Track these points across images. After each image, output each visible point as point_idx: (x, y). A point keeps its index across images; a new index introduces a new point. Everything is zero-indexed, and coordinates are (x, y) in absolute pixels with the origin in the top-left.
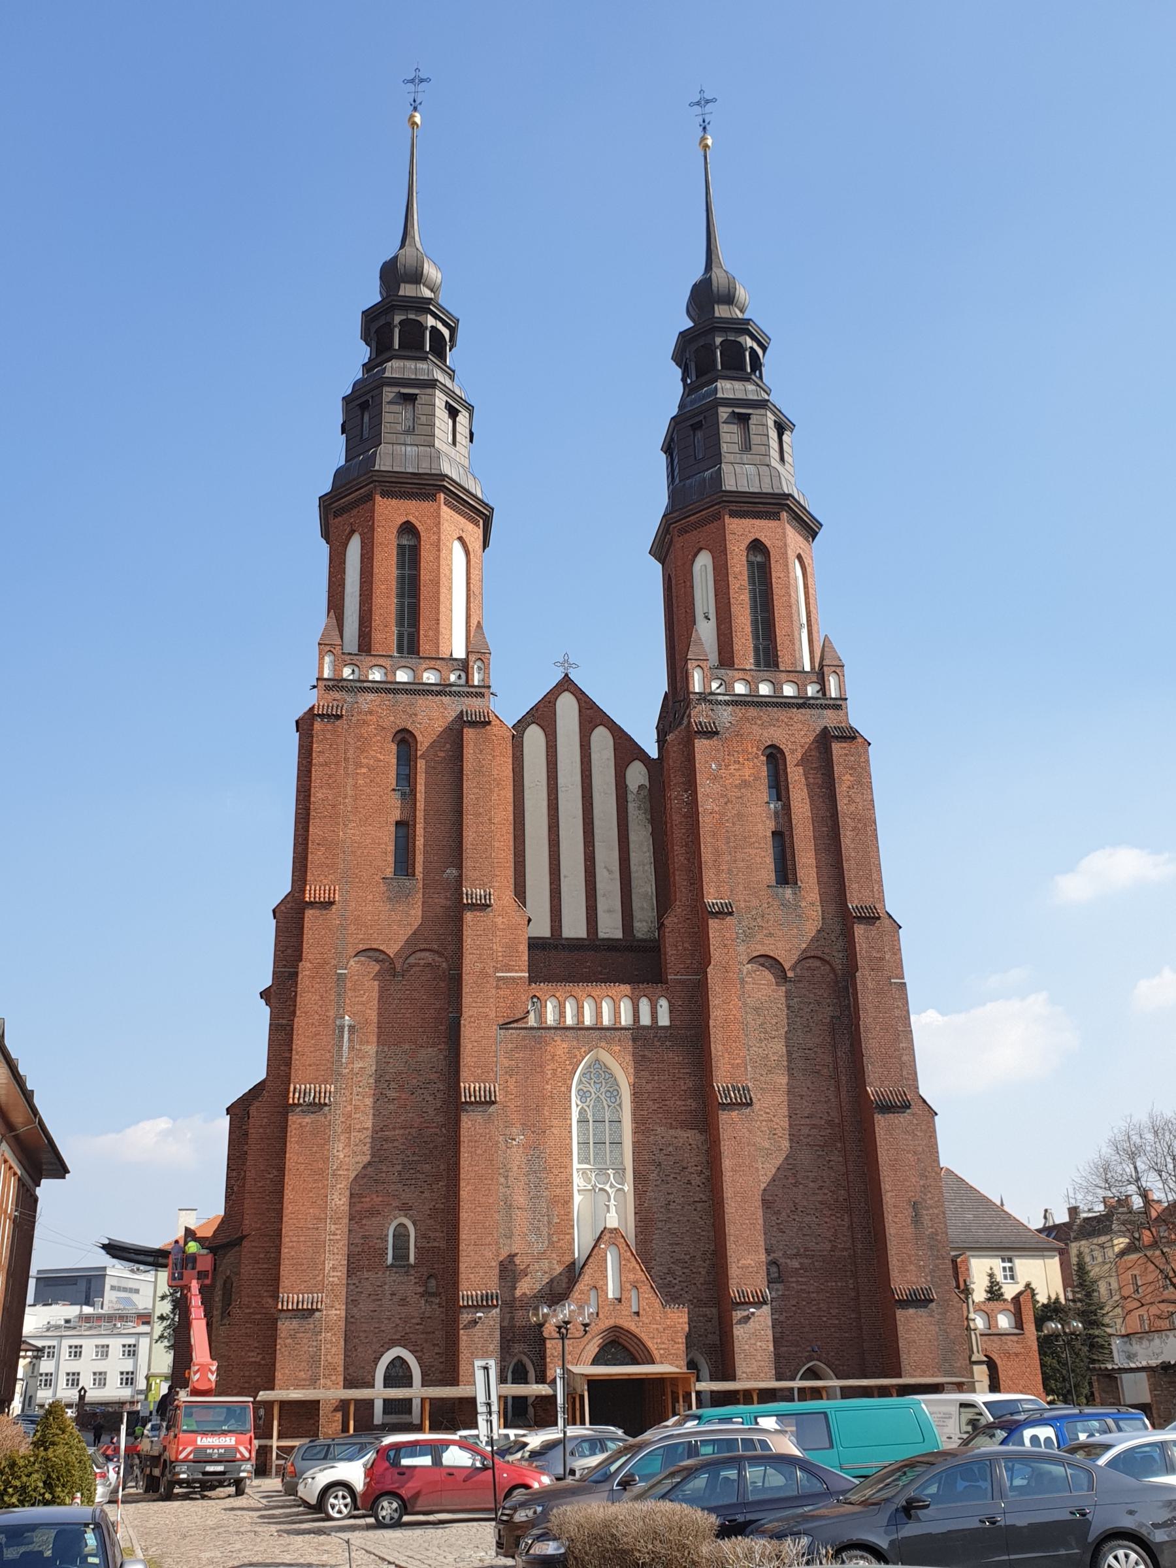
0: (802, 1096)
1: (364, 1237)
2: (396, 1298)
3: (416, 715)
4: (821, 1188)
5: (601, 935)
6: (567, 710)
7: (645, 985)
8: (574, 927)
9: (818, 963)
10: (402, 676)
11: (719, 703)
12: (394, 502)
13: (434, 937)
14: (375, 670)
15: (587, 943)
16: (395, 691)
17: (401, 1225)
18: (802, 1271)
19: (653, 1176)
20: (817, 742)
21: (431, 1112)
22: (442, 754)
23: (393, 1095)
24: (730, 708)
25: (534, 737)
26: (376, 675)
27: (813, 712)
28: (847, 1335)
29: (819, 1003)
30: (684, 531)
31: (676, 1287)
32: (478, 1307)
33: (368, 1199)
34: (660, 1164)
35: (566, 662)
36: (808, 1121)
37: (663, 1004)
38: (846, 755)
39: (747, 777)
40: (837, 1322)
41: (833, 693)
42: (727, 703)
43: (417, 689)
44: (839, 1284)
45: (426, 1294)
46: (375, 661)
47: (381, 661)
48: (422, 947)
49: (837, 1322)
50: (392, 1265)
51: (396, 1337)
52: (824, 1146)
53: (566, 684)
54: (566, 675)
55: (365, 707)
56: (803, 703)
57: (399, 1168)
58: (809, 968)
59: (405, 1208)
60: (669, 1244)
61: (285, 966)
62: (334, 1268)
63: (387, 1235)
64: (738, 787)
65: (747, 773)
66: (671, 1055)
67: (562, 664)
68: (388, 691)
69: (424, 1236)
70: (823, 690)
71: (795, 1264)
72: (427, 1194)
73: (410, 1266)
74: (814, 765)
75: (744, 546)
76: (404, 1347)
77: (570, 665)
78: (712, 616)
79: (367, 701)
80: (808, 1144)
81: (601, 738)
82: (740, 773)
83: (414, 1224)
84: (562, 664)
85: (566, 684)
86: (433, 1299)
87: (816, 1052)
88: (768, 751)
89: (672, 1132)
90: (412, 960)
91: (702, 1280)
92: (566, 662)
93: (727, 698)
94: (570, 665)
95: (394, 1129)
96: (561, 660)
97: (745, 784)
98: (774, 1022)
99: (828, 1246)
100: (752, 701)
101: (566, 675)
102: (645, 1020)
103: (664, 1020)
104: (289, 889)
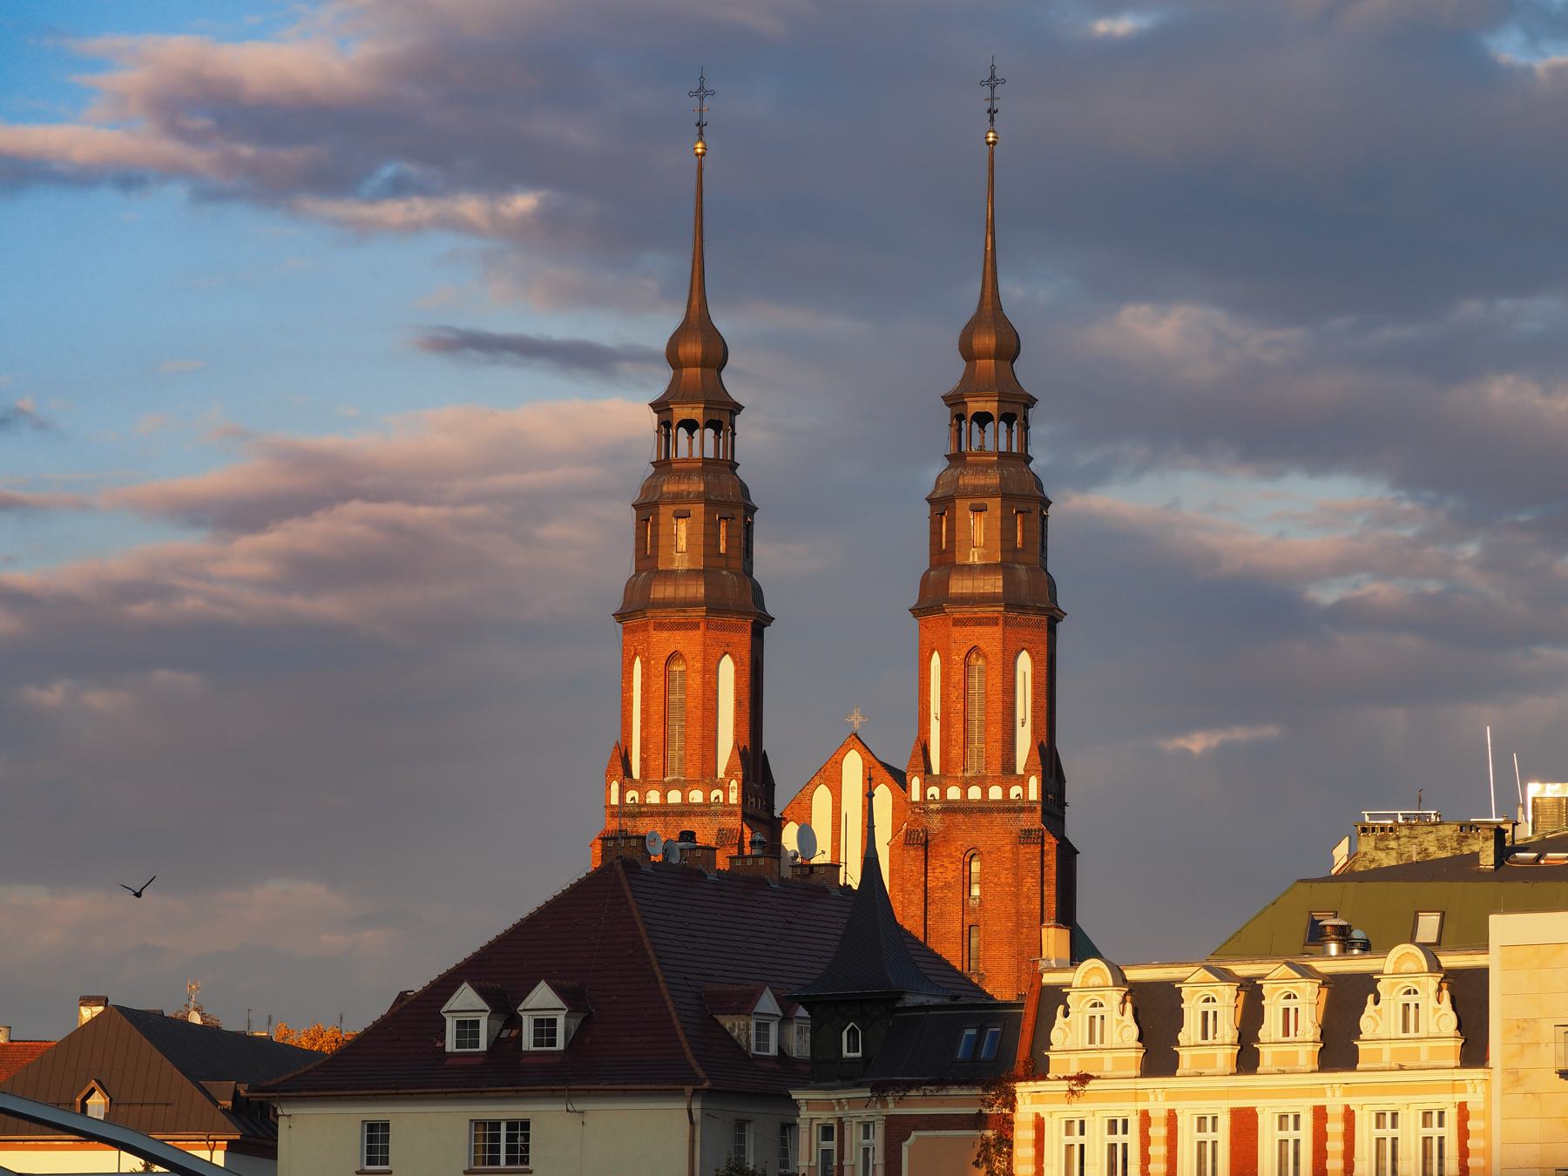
6: (853, 765)
10: (675, 797)
12: (665, 634)
16: (665, 814)
25: (822, 796)
26: (654, 797)
38: (1030, 859)
42: (938, 811)
43: (686, 810)
46: (649, 787)
68: (659, 814)
97: (947, 886)
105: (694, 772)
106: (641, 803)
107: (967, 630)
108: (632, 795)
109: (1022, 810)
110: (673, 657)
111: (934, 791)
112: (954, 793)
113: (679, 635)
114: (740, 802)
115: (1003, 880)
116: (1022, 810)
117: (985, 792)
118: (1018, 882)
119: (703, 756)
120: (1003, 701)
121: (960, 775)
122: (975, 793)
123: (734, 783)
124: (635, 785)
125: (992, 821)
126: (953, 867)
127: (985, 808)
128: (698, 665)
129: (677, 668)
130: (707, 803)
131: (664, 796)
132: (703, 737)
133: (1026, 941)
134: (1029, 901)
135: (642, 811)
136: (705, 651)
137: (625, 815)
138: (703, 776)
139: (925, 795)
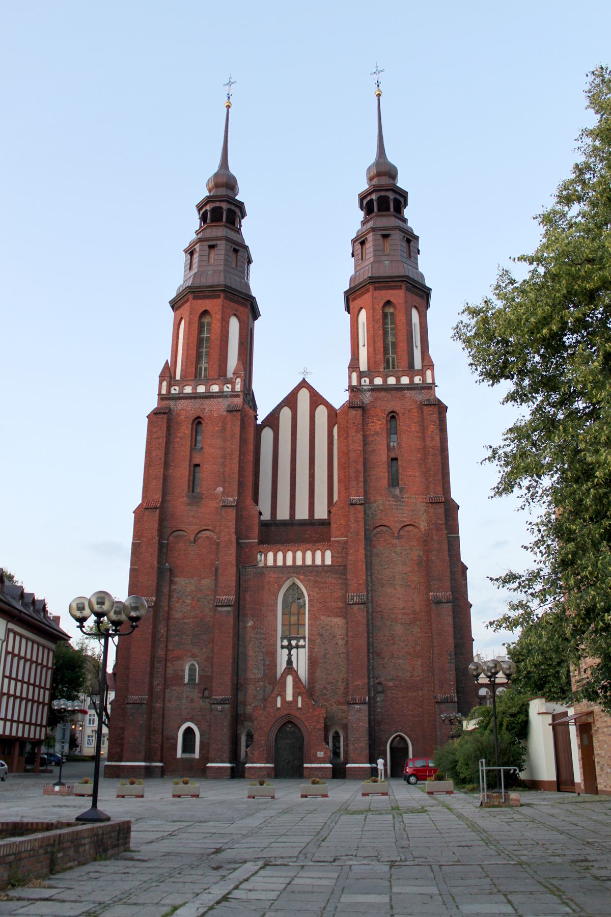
0: (399, 598)
1: (174, 670)
2: (189, 699)
3: (205, 409)
4: (406, 645)
5: (317, 517)
6: (304, 398)
7: (319, 544)
8: (302, 514)
9: (411, 528)
10: (201, 389)
11: (365, 390)
12: (200, 301)
13: (210, 523)
14: (186, 387)
15: (308, 522)
16: (195, 398)
17: (193, 665)
18: (394, 688)
19: (318, 641)
20: (417, 408)
21: (207, 610)
22: (216, 428)
23: (189, 602)
24: (370, 393)
25: (286, 414)
26: (188, 390)
27: (416, 391)
28: (417, 719)
29: (411, 550)
30: (354, 299)
31: (328, 696)
32: (220, 704)
33: (176, 652)
34: (322, 635)
35: (305, 372)
36: (402, 611)
37: (328, 554)
38: (431, 414)
39: (378, 430)
40: (411, 713)
41: (429, 380)
42: (369, 390)
43: (208, 396)
44: (414, 694)
45: (203, 697)
47: (189, 383)
48: (204, 528)
49: (411, 713)
50: (187, 684)
51: (189, 717)
52: (410, 623)
53: (304, 384)
54: (304, 379)
55: (180, 407)
56: (412, 387)
57: (191, 637)
58: (407, 531)
59: (194, 656)
60: (325, 675)
61: (138, 540)
62: (158, 684)
63: (185, 669)
64: (372, 435)
65: (377, 427)
66: (330, 579)
67: (303, 373)
69: (203, 670)
70: (424, 380)
71: (391, 684)
72: (204, 650)
73: (196, 684)
74: (415, 421)
75: (381, 305)
76: (192, 722)
77: (307, 373)
78: (366, 344)
79: (182, 404)
80: (401, 623)
81: (321, 411)
82: (374, 427)
83: (198, 664)
84: (303, 373)
85: (304, 384)
86: (206, 700)
87: (408, 575)
88: (391, 415)
89: (329, 619)
90: (199, 535)
91: (341, 692)
92: (305, 372)
93: (369, 387)
94: (307, 373)
95: (189, 618)
96: (303, 371)
97: (377, 433)
98: (386, 560)
99: (409, 674)
100: (385, 388)
101: (304, 379)
102: (318, 562)
103: (328, 562)
104: (140, 502)
105: (214, 373)
106: (181, 392)
107: (383, 292)
108: (175, 390)
109: (423, 388)
110: (205, 313)
111: (366, 381)
112: (378, 381)
113: (207, 302)
114: (243, 390)
115: (413, 429)
116: (423, 388)
117: (398, 380)
118: (423, 428)
119: (220, 365)
120: (407, 329)
121: (382, 370)
122: (392, 381)
123: (239, 380)
124: (177, 383)
125: (403, 396)
126: (380, 422)
127: (399, 388)
128: (219, 317)
129: (206, 320)
130: (221, 391)
131: (195, 388)
132: (220, 355)
133: (433, 464)
134: (433, 439)
135: (182, 397)
136: (223, 309)
137: (169, 399)
138: (219, 376)
139: (360, 382)
